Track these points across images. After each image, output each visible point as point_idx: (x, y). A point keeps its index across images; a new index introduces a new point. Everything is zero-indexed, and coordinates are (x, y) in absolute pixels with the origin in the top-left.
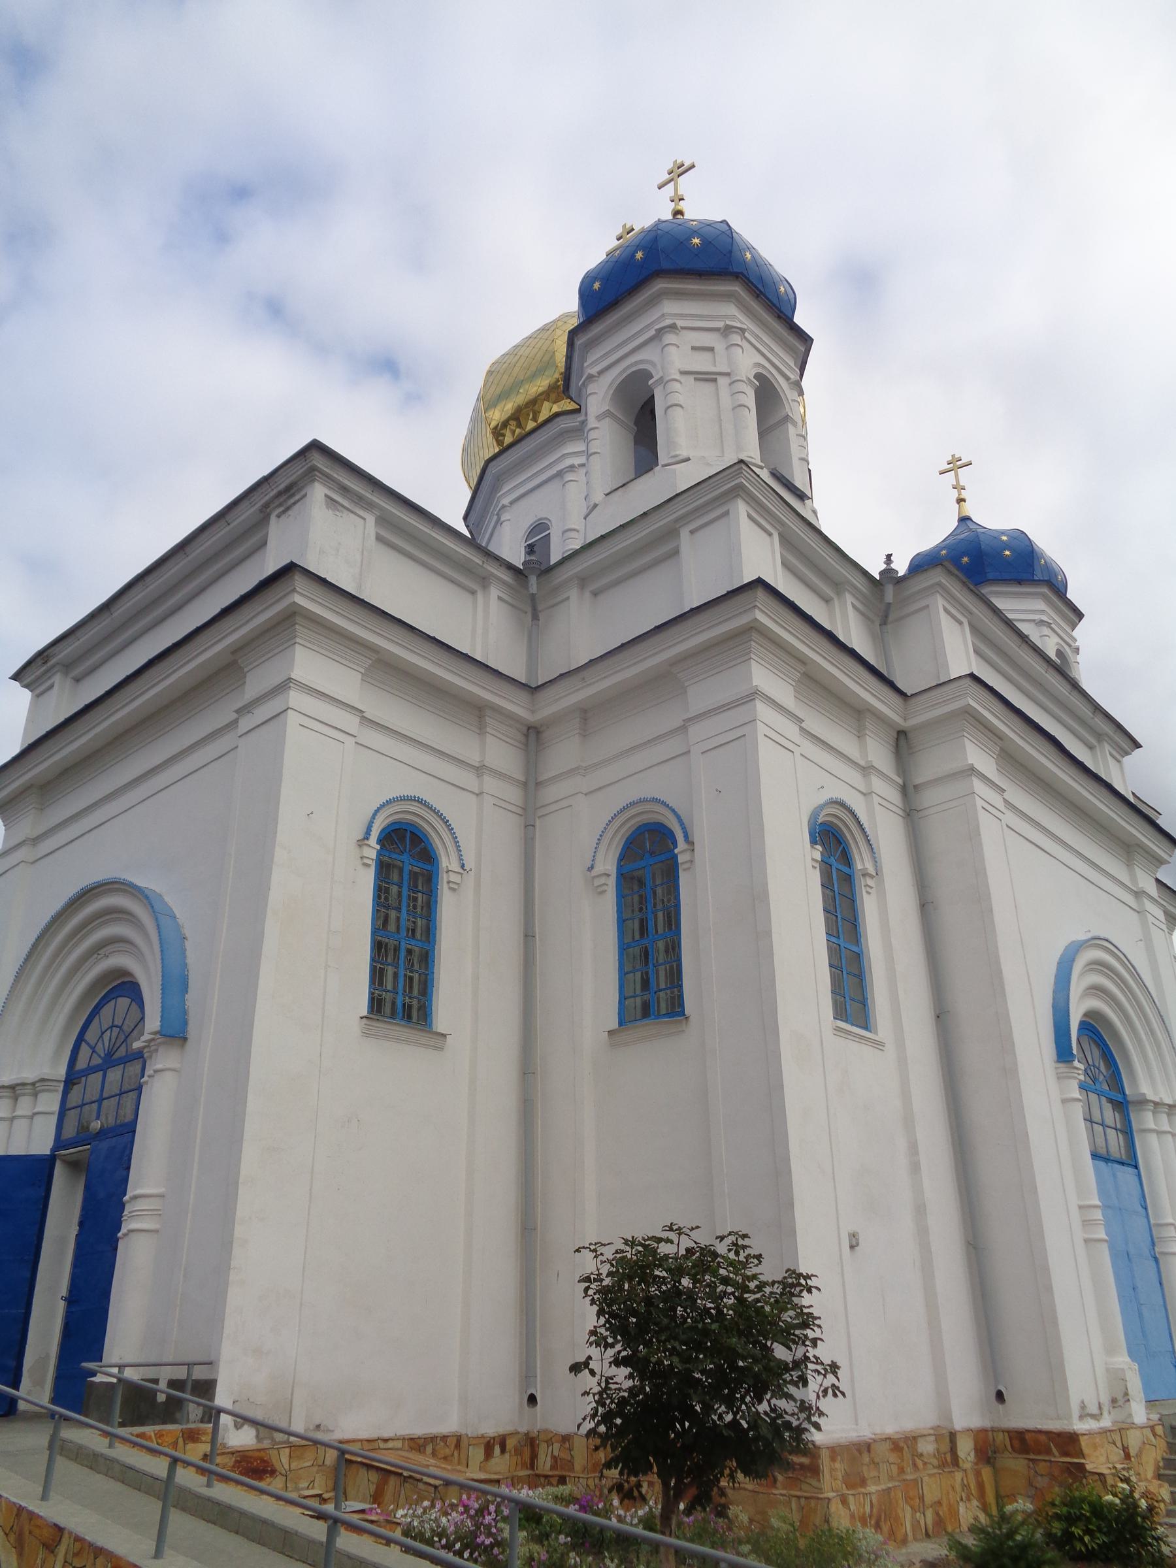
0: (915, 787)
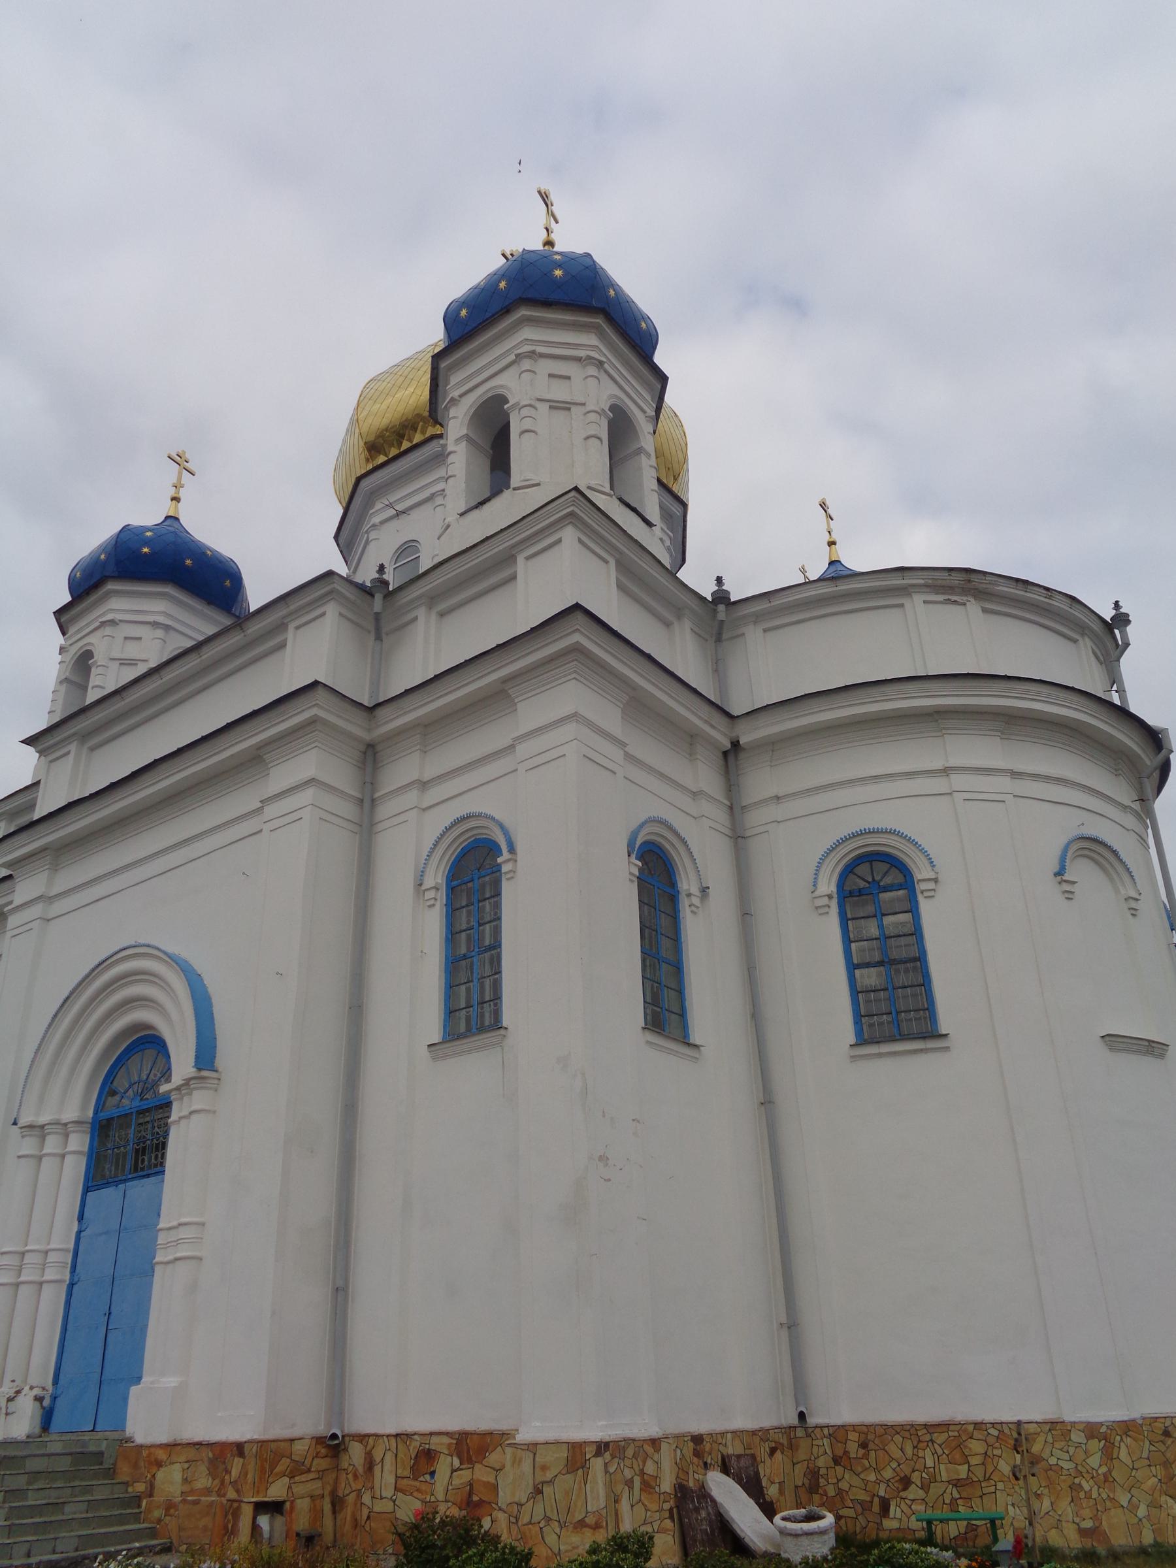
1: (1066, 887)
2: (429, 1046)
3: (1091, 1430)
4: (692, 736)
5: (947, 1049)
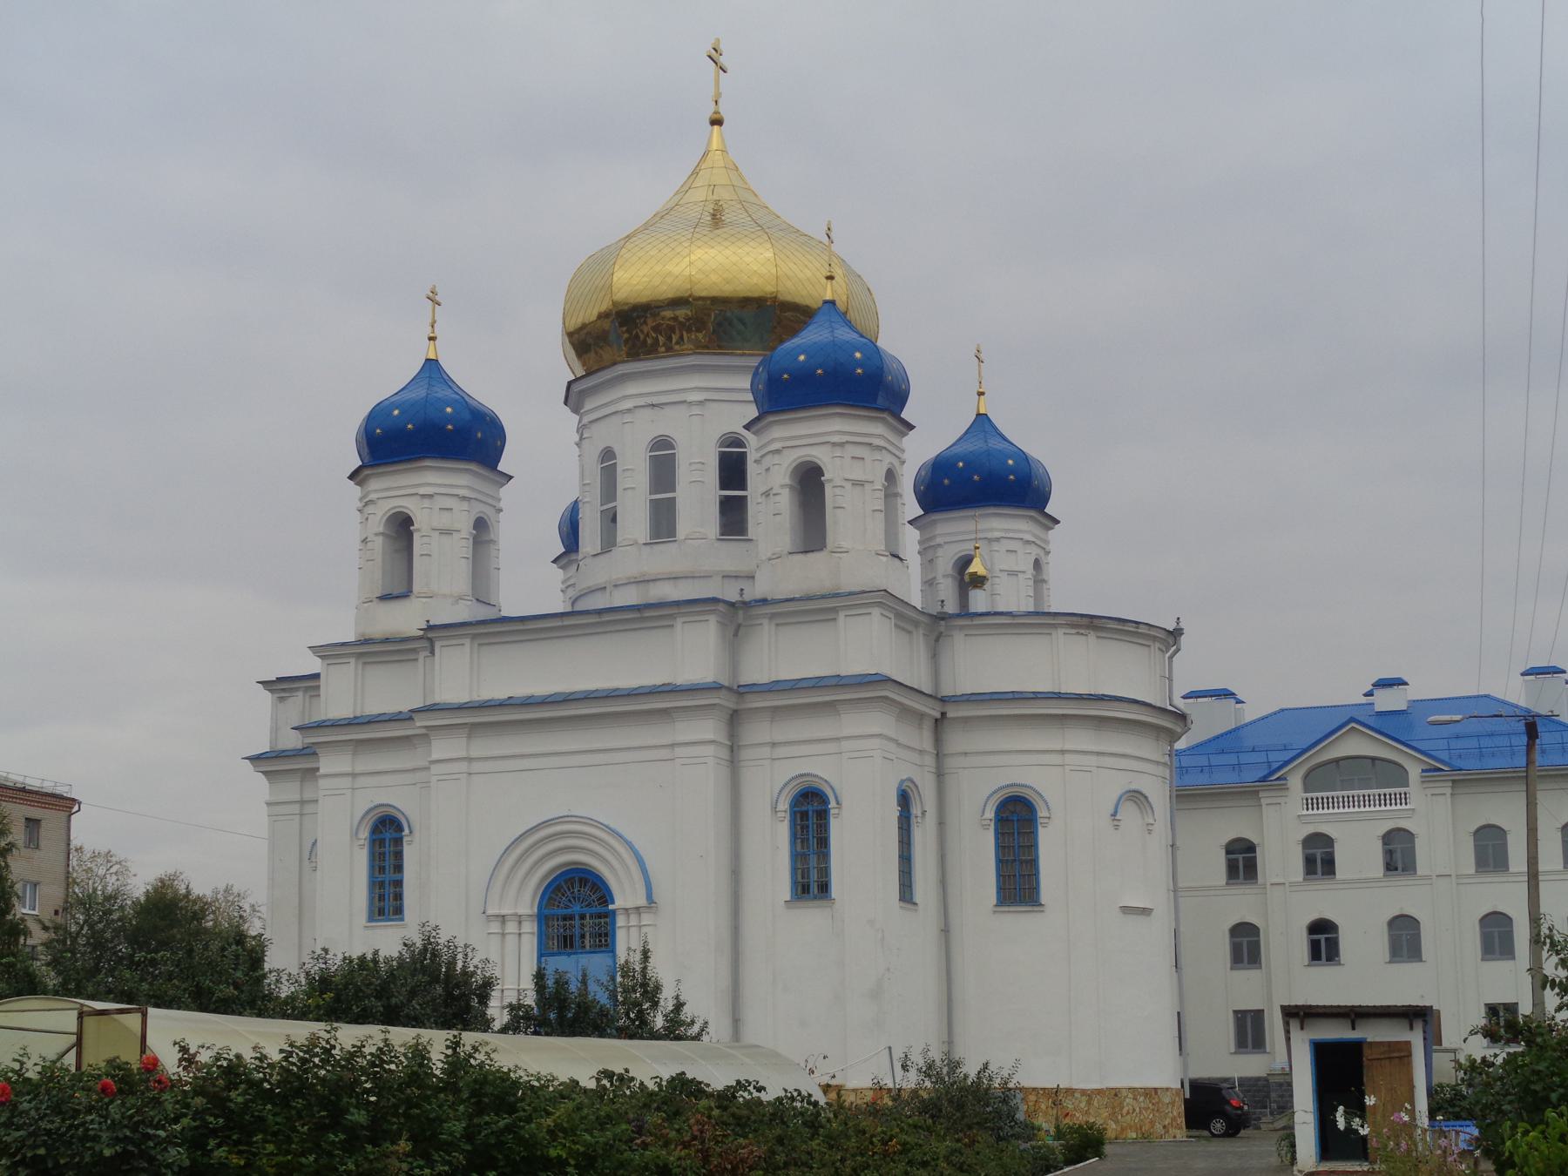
0: (945, 755)
1: (1116, 823)
2: (786, 901)
3: (1083, 1092)
4: (922, 715)
5: (1043, 911)
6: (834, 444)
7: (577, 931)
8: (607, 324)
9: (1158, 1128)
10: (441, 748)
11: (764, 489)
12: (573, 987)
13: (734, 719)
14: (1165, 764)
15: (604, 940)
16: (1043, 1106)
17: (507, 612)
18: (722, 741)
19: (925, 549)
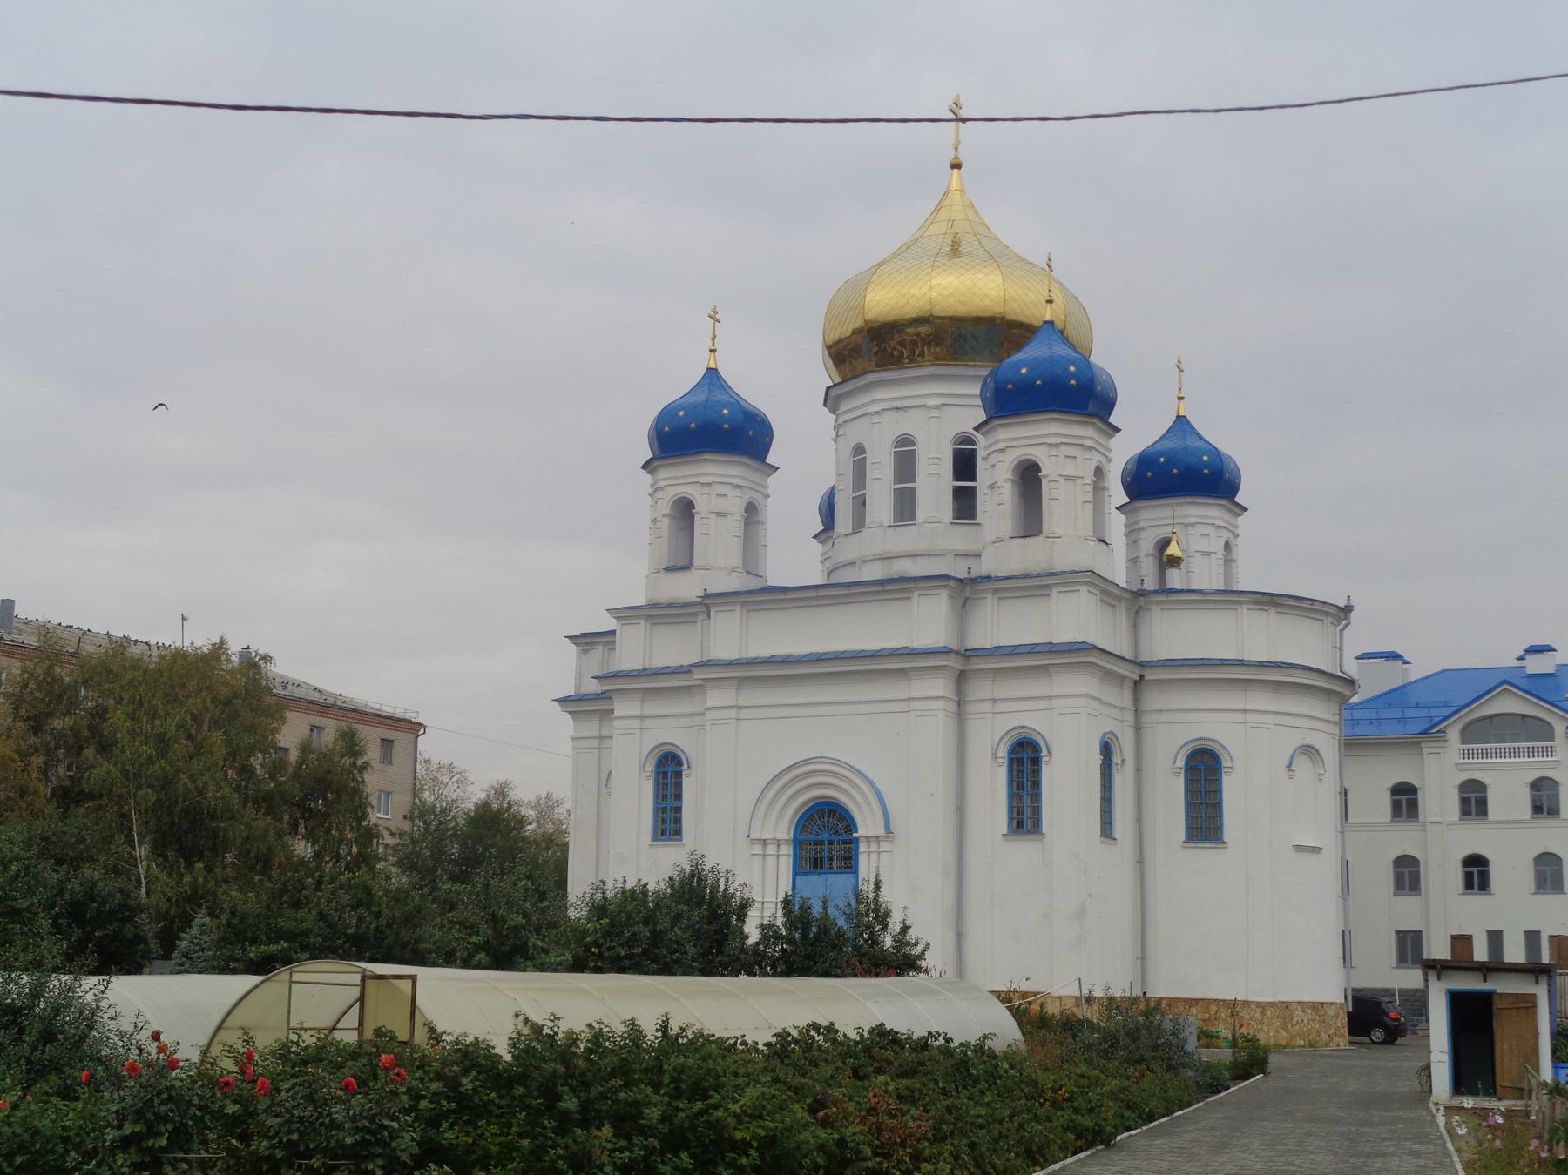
1: (1291, 773)
3: (1258, 1004)
6: (1050, 445)
7: (826, 854)
8: (859, 339)
9: (1324, 1036)
10: (715, 697)
11: (989, 482)
12: (817, 910)
13: (961, 678)
14: (1335, 723)
15: (849, 862)
16: (1223, 1015)
17: (773, 581)
18: (952, 697)
19: (1130, 532)
